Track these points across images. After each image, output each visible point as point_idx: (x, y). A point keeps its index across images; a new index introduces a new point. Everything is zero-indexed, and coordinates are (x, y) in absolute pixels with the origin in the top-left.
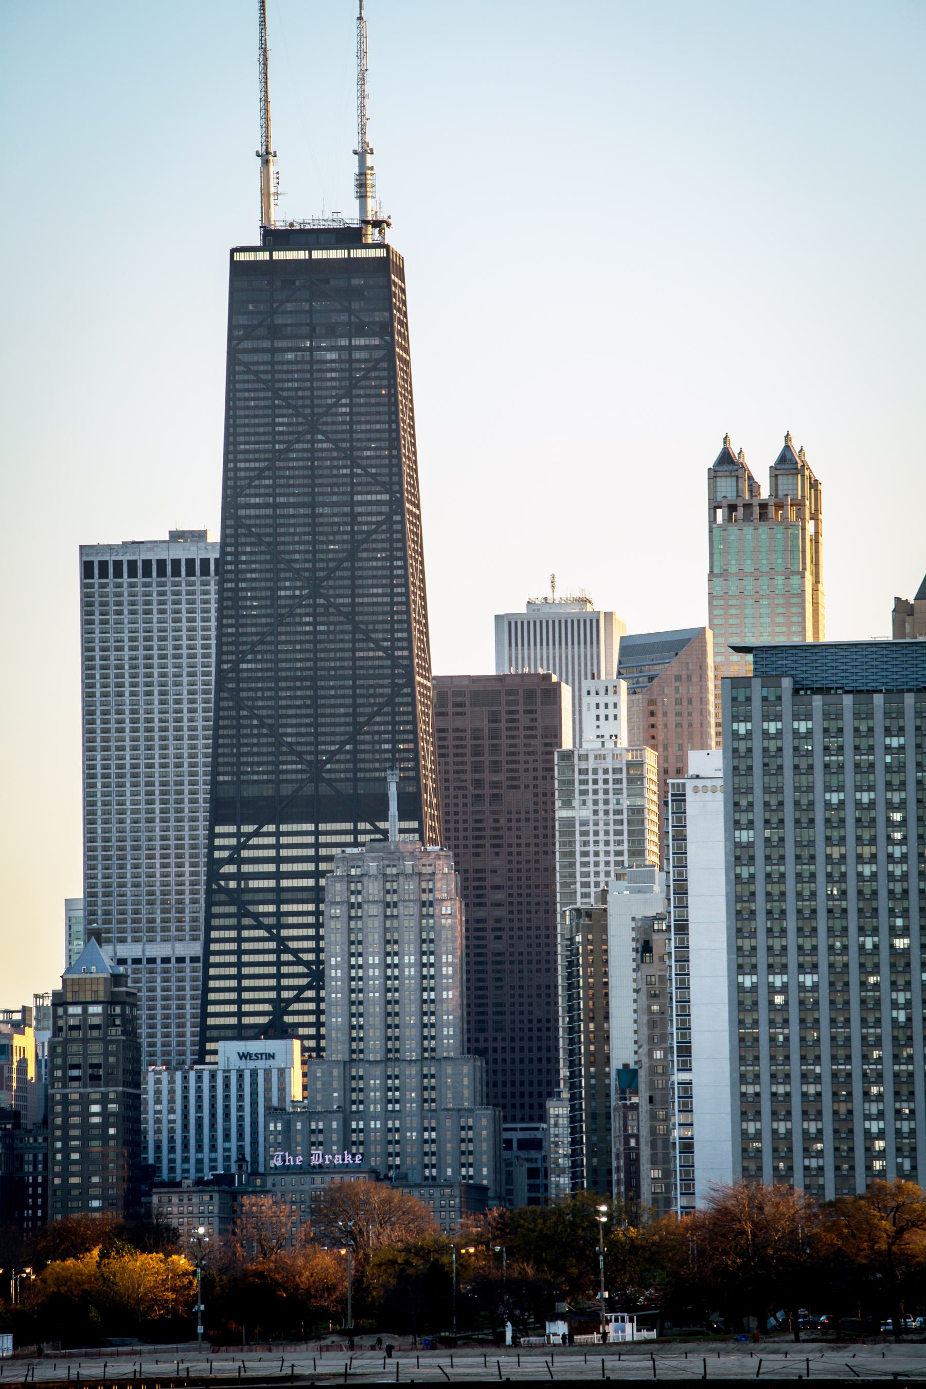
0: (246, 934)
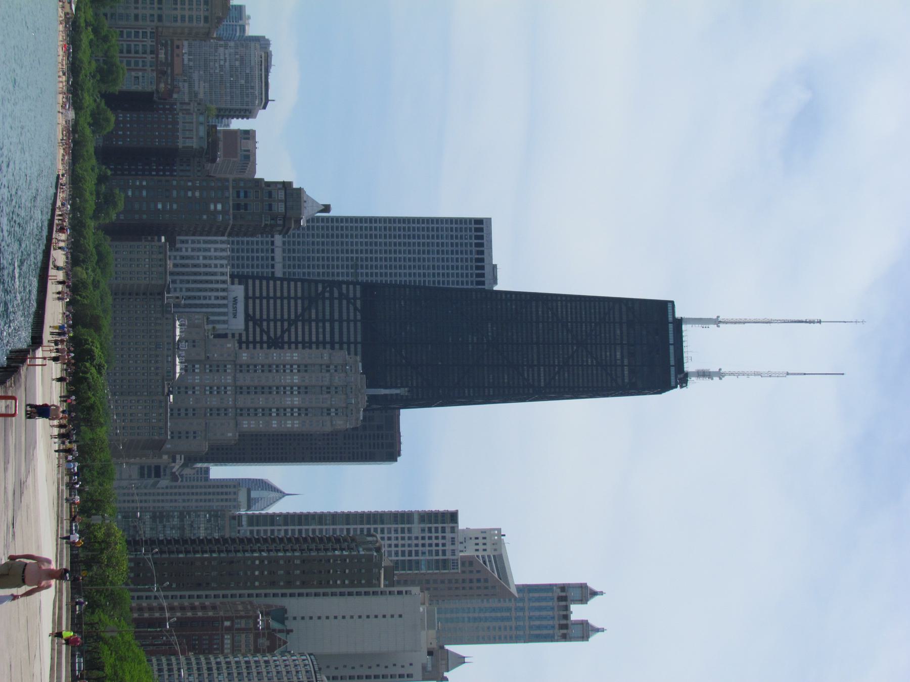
0: (299, 302)
